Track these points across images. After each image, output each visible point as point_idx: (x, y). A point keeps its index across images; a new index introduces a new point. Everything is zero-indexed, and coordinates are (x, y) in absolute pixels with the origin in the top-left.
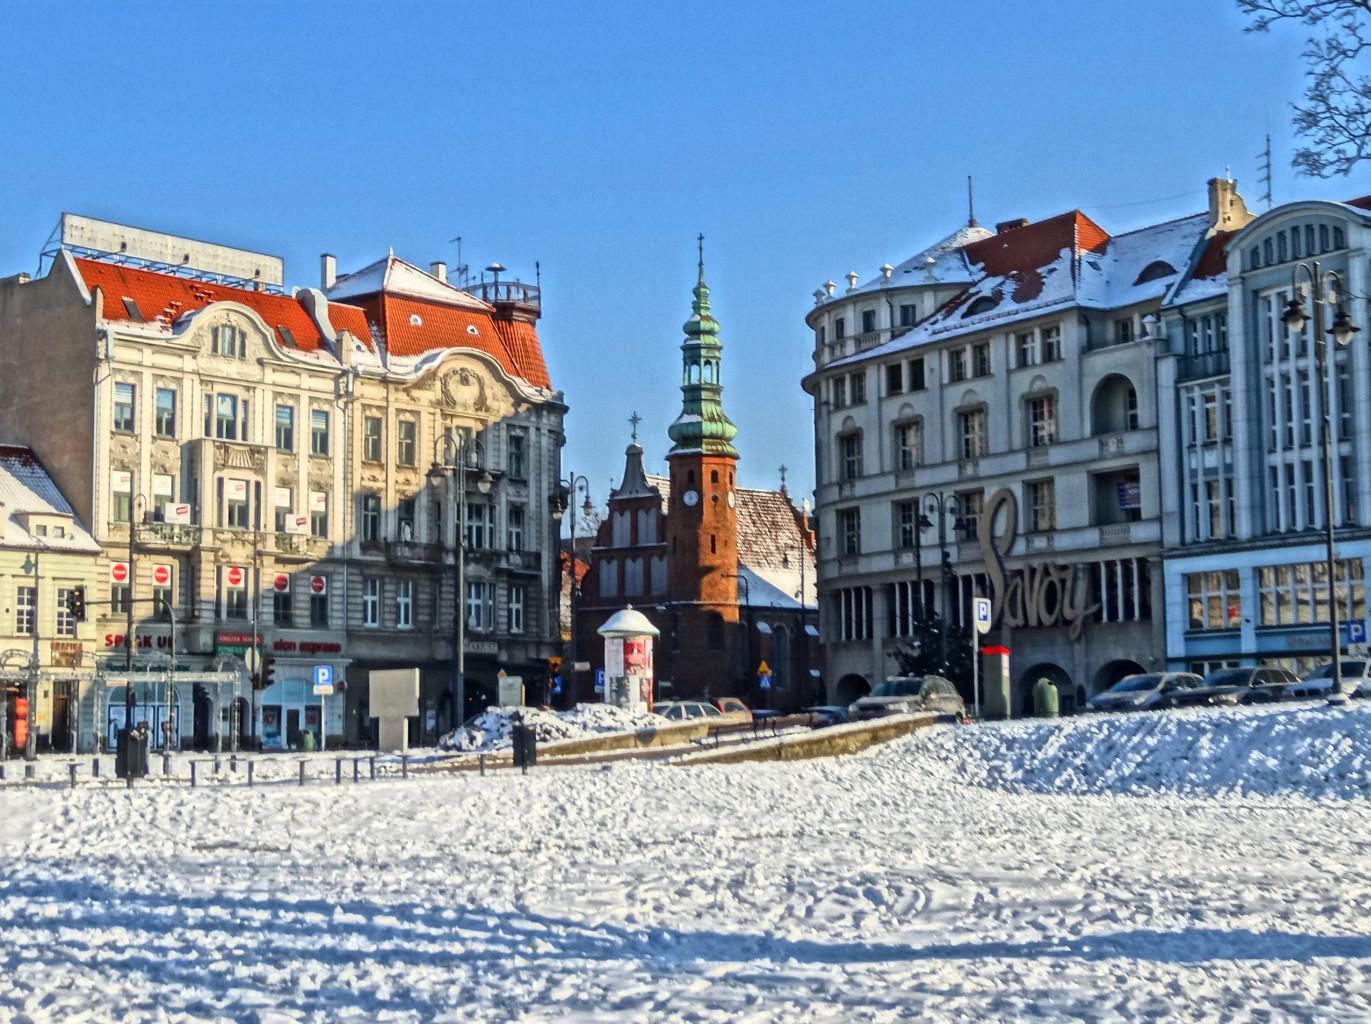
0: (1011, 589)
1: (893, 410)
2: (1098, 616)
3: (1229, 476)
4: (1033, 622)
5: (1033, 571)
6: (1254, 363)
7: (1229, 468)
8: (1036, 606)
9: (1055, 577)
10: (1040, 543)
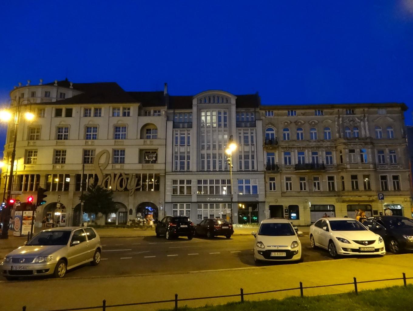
2: (139, 189)
3: (188, 155)
5: (115, 175)
7: (189, 153)
9: (124, 177)
10: (118, 166)
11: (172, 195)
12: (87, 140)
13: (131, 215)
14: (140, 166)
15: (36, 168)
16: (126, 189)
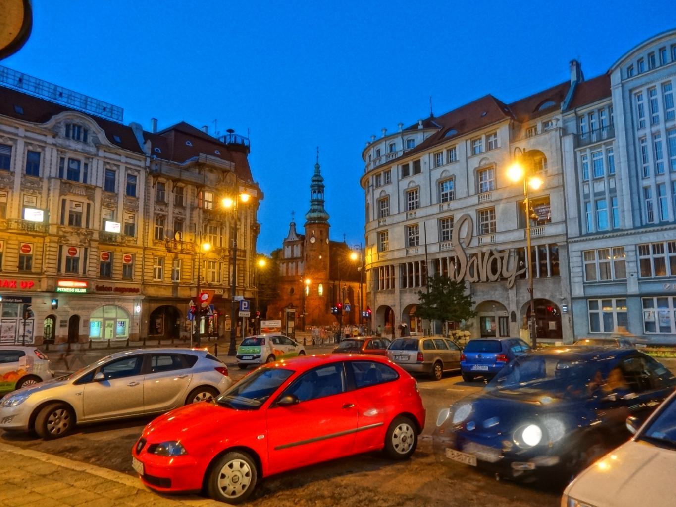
0: (470, 264)
1: (405, 184)
2: (523, 276)
4: (484, 278)
5: (483, 254)
6: (631, 128)
7: (613, 191)
8: (485, 270)
9: (497, 256)
10: (487, 239)
11: (584, 283)
12: (442, 204)
13: (514, 323)
14: (519, 235)
15: (390, 256)
16: (503, 279)
